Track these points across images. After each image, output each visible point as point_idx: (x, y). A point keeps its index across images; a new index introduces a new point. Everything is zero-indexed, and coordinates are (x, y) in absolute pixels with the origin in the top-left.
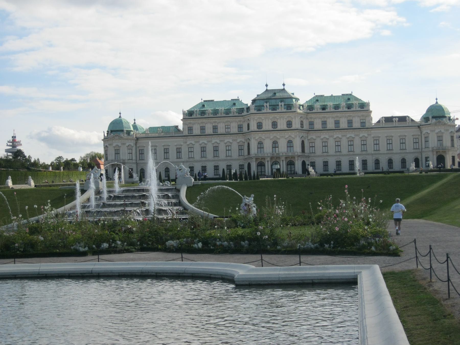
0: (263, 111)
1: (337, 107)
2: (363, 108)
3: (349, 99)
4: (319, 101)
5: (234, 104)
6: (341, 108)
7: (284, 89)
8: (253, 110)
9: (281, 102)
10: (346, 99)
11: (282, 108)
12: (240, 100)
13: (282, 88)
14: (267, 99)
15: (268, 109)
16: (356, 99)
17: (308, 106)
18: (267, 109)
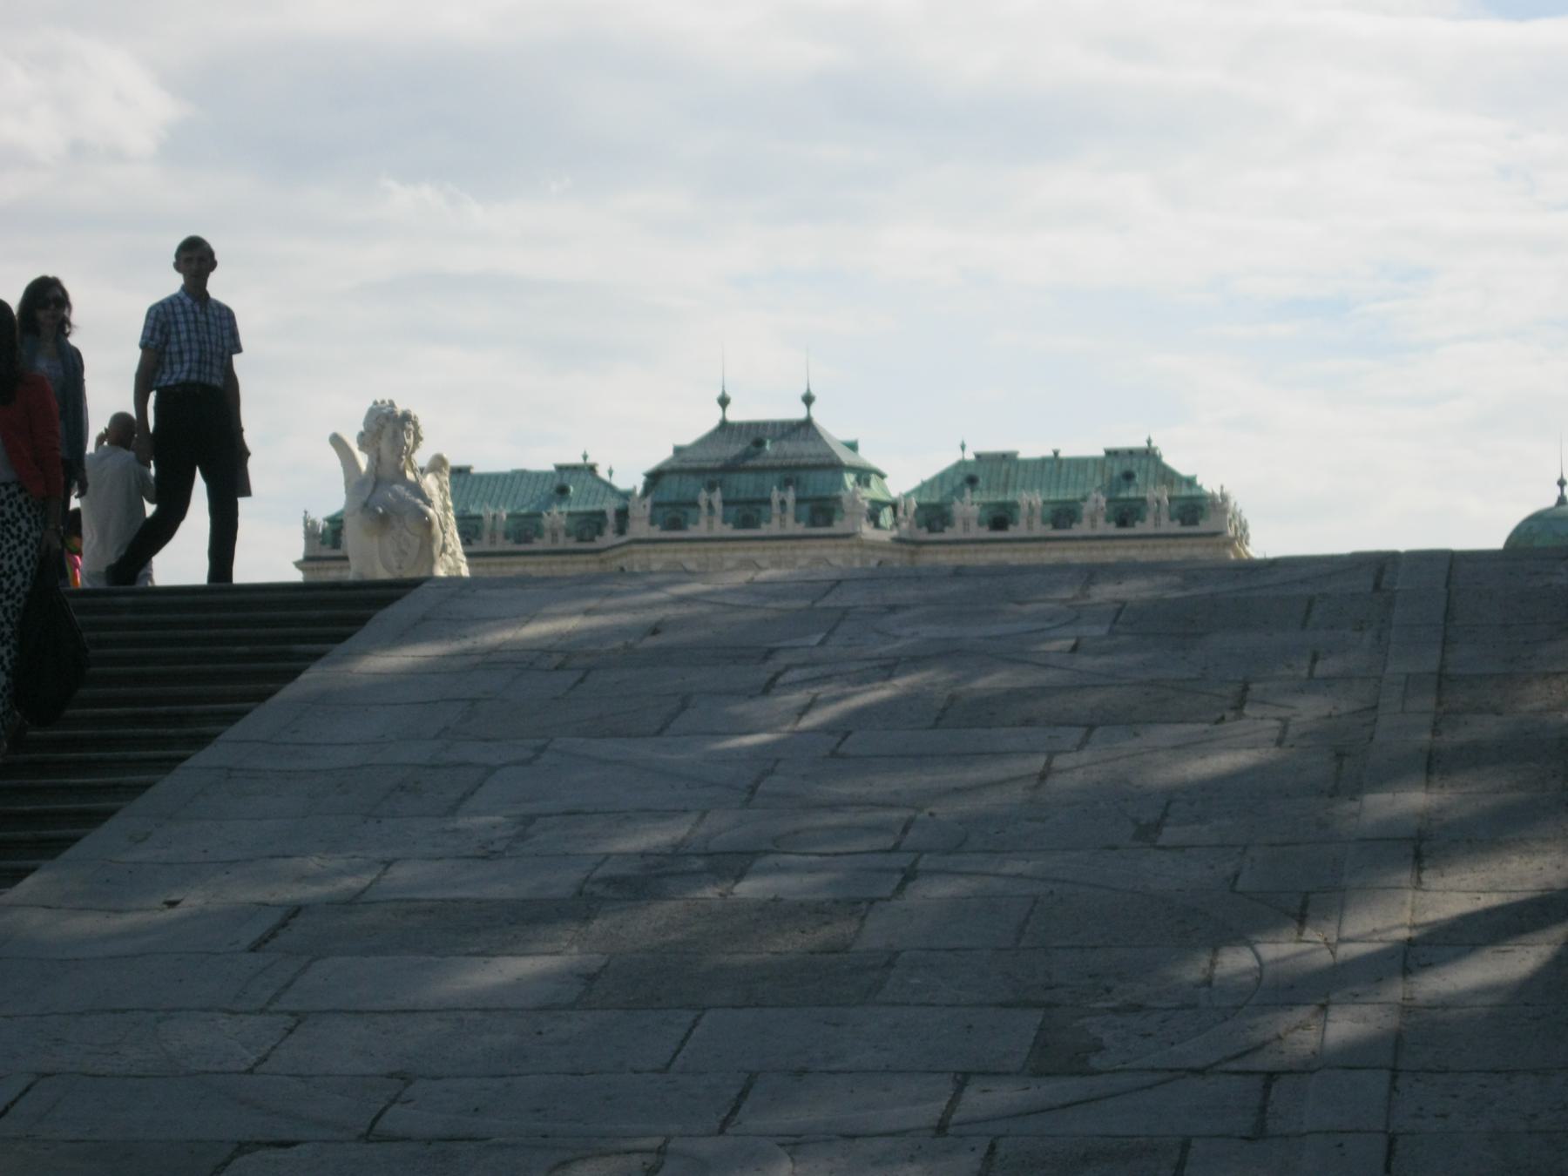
0: (693, 531)
1: (1063, 515)
2: (1194, 522)
3: (1128, 476)
4: (982, 483)
5: (562, 490)
6: (1086, 523)
7: (807, 424)
8: (645, 524)
9: (785, 484)
10: (1117, 473)
11: (783, 520)
12: (602, 473)
13: (799, 413)
14: (713, 471)
15: (717, 522)
16: (1168, 476)
17: (920, 506)
18: (710, 523)
